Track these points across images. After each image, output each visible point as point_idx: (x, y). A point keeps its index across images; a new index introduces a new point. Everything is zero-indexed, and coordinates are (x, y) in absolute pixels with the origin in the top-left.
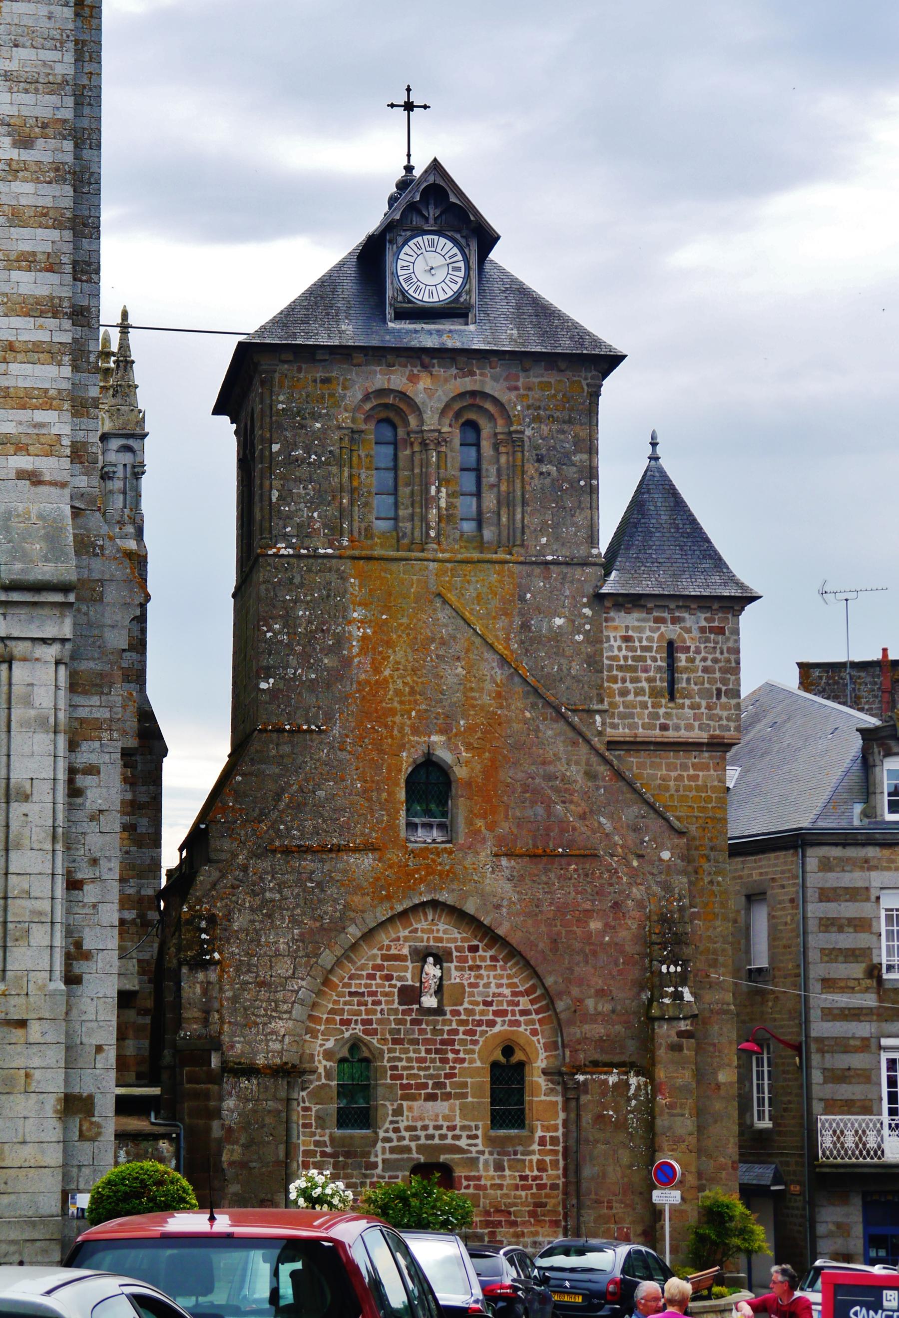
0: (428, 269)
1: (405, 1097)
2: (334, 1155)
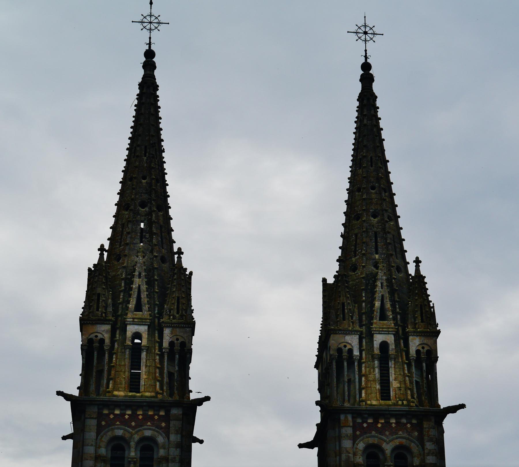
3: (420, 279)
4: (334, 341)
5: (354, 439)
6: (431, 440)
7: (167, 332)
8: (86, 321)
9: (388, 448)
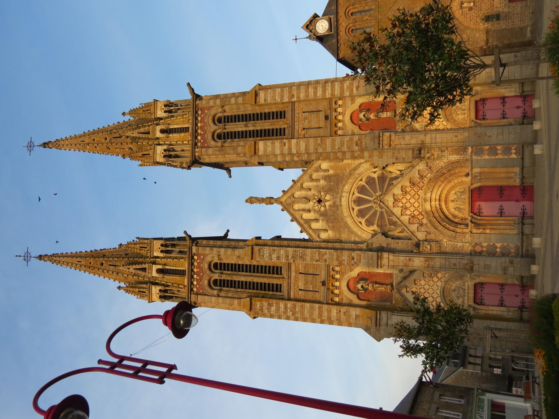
0: (322, 27)
1: (493, 6)
2: (506, 20)
3: (133, 112)
4: (160, 159)
5: (209, 147)
6: (208, 102)
7: (156, 254)
8: (151, 301)
9: (213, 127)
